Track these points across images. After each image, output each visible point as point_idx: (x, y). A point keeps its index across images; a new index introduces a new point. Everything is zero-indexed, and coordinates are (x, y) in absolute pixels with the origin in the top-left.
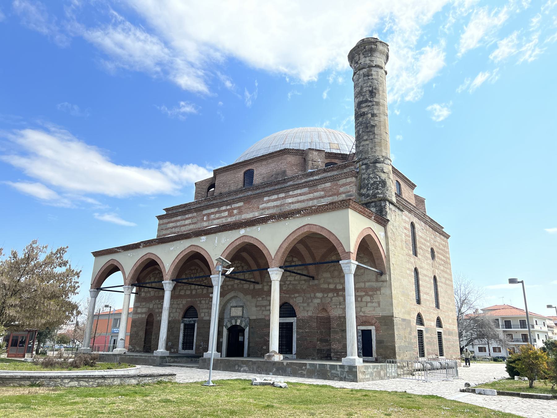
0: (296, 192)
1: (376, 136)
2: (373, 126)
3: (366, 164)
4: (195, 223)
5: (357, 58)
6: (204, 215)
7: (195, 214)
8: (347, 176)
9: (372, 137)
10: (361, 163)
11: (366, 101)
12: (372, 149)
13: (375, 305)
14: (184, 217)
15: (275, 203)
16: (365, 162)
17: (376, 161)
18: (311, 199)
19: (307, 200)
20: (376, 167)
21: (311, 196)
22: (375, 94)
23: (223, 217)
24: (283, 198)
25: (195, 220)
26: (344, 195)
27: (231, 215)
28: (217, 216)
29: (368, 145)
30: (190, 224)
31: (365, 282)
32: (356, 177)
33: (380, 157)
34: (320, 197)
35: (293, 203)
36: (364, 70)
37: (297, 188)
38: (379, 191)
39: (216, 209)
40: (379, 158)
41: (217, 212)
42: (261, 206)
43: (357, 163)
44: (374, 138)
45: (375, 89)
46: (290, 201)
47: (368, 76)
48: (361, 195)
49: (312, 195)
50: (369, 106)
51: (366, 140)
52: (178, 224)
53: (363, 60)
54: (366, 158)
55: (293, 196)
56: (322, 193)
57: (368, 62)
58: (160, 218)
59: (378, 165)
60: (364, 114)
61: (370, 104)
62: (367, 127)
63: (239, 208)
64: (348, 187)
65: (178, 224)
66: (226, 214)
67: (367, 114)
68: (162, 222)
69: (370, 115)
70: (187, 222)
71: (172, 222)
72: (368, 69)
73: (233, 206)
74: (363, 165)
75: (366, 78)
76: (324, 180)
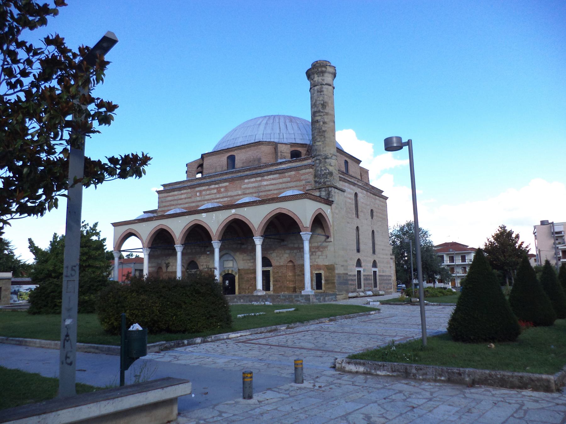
0: (270, 177)
2: (324, 131)
4: (190, 198)
7: (189, 190)
8: (306, 167)
9: (323, 139)
11: (319, 111)
12: (323, 148)
13: (324, 257)
14: (180, 192)
15: (254, 185)
16: (319, 157)
21: (281, 181)
23: (213, 194)
24: (260, 181)
25: (189, 195)
26: (304, 182)
27: (219, 192)
28: (208, 192)
30: (185, 198)
31: (317, 242)
35: (267, 185)
39: (207, 187)
41: (207, 190)
42: (243, 186)
44: (325, 140)
45: (326, 102)
47: (321, 92)
48: (316, 182)
49: (281, 180)
51: (319, 142)
52: (176, 198)
53: (317, 78)
55: (267, 180)
57: (320, 81)
58: (159, 192)
60: (318, 121)
61: (322, 114)
62: (320, 132)
63: (226, 187)
64: (307, 176)
66: (215, 191)
69: (321, 123)
70: (183, 196)
73: (221, 185)
76: (291, 169)
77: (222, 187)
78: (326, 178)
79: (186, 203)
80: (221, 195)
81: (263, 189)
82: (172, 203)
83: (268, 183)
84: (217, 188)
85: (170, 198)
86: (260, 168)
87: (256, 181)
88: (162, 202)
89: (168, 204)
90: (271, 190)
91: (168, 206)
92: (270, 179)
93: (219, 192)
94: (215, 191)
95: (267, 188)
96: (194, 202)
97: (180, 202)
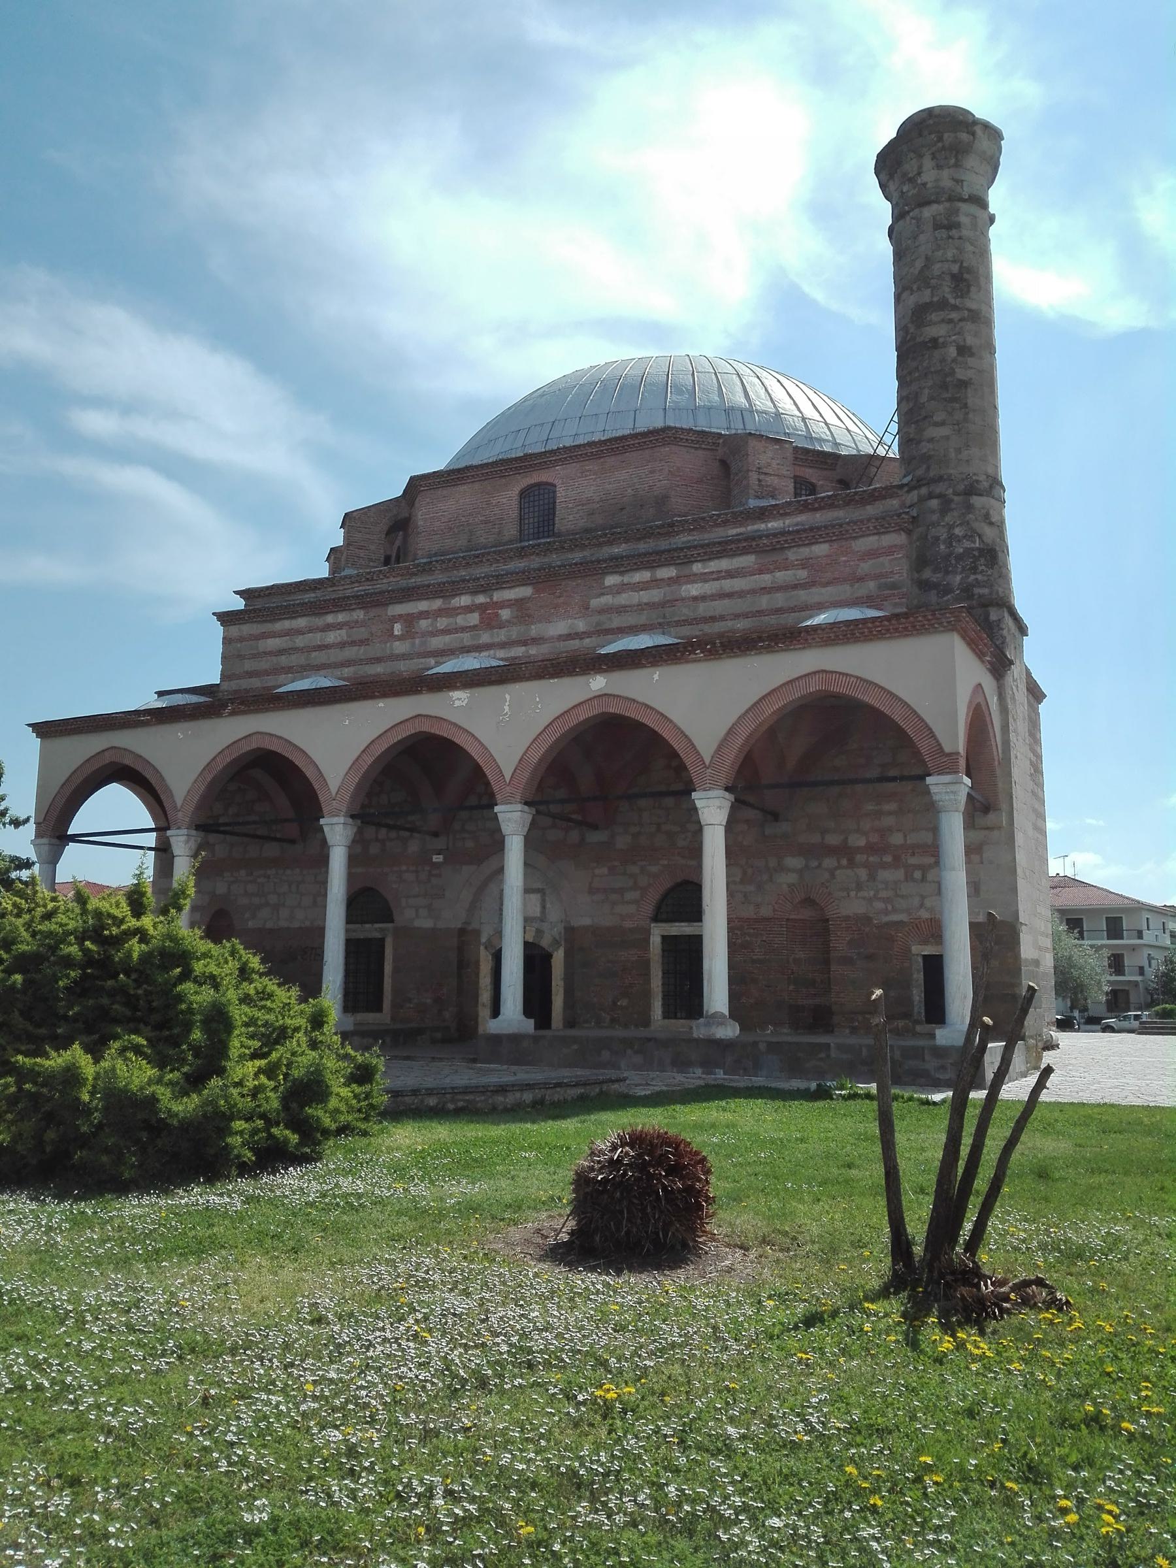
1: (971, 416)
2: (964, 384)
3: (939, 496)
5: (910, 166)
6: (394, 619)
7: (359, 615)
9: (959, 415)
10: (924, 491)
11: (943, 305)
12: (959, 451)
14: (319, 621)
15: (645, 596)
16: (939, 488)
17: (972, 490)
18: (765, 590)
19: (753, 592)
20: (969, 507)
21: (766, 579)
22: (969, 286)
24: (672, 581)
25: (361, 633)
26: (872, 585)
27: (490, 621)
28: (442, 623)
29: (947, 438)
30: (342, 645)
32: (909, 532)
33: (982, 478)
34: (795, 587)
35: (703, 598)
36: (935, 207)
37: (719, 555)
38: (979, 577)
39: (437, 604)
40: (977, 481)
41: (440, 613)
42: (595, 603)
43: (908, 492)
44: (966, 420)
45: (969, 270)
46: (694, 593)
50: (950, 321)
51: (942, 424)
52: (300, 641)
54: (940, 479)
55: (704, 578)
56: (803, 574)
57: (947, 183)
58: (226, 618)
59: (977, 501)
60: (934, 343)
61: (954, 315)
63: (519, 603)
64: (885, 560)
65: (300, 641)
66: (474, 618)
67: (944, 345)
68: (235, 630)
69: (952, 351)
70: (332, 637)
71: (273, 635)
72: (947, 205)
73: (497, 596)
74: (931, 496)
75: (943, 233)
76: (812, 535)
77: (502, 605)
78: (974, 570)
79: (348, 663)
80: (502, 635)
81: (685, 612)
82: (284, 660)
83: (709, 588)
84: (482, 608)
85: (272, 643)
86: (671, 529)
87: (655, 583)
88: (241, 657)
89: (264, 664)
90: (722, 618)
91: (267, 673)
92: (719, 576)
93: (490, 621)
94: (474, 618)
95: (703, 609)
96: (378, 660)
97: (318, 657)
